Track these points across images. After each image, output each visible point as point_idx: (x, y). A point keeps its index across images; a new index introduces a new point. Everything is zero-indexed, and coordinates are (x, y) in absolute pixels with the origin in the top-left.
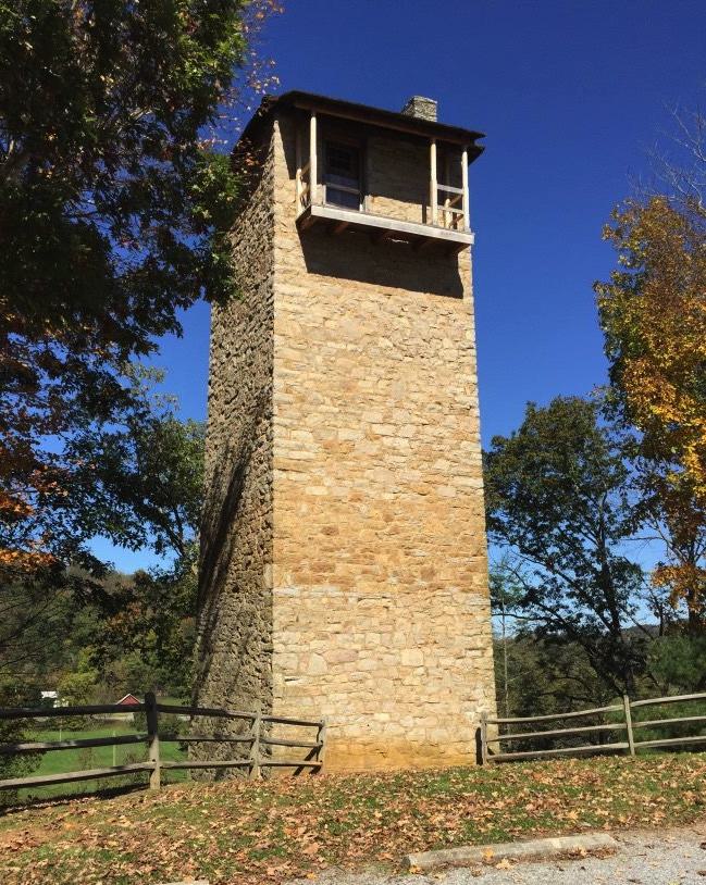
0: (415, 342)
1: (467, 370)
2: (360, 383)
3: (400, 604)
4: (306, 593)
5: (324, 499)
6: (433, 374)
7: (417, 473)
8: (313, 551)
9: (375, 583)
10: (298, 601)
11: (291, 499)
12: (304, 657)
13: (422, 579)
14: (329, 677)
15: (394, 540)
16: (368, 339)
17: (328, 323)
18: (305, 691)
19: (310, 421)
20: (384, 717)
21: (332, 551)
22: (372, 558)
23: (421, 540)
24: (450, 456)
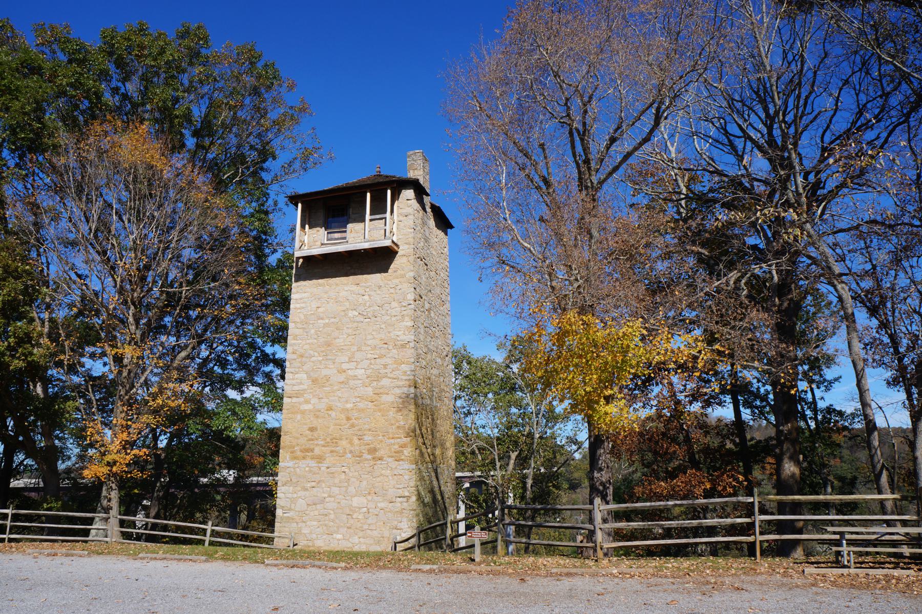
0: (372, 308)
1: (407, 319)
2: (338, 341)
3: (352, 469)
4: (296, 465)
5: (310, 411)
6: (383, 326)
7: (370, 389)
8: (302, 441)
9: (338, 458)
10: (292, 470)
11: (292, 413)
12: (293, 501)
13: (369, 454)
14: (307, 512)
15: (350, 432)
16: (343, 314)
17: (320, 310)
18: (293, 519)
19: (305, 368)
20: (339, 536)
21: (312, 440)
22: (336, 443)
23: (370, 430)
24: (392, 376)
